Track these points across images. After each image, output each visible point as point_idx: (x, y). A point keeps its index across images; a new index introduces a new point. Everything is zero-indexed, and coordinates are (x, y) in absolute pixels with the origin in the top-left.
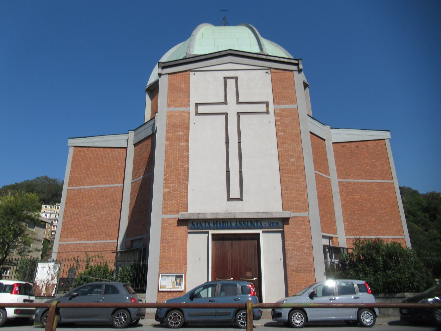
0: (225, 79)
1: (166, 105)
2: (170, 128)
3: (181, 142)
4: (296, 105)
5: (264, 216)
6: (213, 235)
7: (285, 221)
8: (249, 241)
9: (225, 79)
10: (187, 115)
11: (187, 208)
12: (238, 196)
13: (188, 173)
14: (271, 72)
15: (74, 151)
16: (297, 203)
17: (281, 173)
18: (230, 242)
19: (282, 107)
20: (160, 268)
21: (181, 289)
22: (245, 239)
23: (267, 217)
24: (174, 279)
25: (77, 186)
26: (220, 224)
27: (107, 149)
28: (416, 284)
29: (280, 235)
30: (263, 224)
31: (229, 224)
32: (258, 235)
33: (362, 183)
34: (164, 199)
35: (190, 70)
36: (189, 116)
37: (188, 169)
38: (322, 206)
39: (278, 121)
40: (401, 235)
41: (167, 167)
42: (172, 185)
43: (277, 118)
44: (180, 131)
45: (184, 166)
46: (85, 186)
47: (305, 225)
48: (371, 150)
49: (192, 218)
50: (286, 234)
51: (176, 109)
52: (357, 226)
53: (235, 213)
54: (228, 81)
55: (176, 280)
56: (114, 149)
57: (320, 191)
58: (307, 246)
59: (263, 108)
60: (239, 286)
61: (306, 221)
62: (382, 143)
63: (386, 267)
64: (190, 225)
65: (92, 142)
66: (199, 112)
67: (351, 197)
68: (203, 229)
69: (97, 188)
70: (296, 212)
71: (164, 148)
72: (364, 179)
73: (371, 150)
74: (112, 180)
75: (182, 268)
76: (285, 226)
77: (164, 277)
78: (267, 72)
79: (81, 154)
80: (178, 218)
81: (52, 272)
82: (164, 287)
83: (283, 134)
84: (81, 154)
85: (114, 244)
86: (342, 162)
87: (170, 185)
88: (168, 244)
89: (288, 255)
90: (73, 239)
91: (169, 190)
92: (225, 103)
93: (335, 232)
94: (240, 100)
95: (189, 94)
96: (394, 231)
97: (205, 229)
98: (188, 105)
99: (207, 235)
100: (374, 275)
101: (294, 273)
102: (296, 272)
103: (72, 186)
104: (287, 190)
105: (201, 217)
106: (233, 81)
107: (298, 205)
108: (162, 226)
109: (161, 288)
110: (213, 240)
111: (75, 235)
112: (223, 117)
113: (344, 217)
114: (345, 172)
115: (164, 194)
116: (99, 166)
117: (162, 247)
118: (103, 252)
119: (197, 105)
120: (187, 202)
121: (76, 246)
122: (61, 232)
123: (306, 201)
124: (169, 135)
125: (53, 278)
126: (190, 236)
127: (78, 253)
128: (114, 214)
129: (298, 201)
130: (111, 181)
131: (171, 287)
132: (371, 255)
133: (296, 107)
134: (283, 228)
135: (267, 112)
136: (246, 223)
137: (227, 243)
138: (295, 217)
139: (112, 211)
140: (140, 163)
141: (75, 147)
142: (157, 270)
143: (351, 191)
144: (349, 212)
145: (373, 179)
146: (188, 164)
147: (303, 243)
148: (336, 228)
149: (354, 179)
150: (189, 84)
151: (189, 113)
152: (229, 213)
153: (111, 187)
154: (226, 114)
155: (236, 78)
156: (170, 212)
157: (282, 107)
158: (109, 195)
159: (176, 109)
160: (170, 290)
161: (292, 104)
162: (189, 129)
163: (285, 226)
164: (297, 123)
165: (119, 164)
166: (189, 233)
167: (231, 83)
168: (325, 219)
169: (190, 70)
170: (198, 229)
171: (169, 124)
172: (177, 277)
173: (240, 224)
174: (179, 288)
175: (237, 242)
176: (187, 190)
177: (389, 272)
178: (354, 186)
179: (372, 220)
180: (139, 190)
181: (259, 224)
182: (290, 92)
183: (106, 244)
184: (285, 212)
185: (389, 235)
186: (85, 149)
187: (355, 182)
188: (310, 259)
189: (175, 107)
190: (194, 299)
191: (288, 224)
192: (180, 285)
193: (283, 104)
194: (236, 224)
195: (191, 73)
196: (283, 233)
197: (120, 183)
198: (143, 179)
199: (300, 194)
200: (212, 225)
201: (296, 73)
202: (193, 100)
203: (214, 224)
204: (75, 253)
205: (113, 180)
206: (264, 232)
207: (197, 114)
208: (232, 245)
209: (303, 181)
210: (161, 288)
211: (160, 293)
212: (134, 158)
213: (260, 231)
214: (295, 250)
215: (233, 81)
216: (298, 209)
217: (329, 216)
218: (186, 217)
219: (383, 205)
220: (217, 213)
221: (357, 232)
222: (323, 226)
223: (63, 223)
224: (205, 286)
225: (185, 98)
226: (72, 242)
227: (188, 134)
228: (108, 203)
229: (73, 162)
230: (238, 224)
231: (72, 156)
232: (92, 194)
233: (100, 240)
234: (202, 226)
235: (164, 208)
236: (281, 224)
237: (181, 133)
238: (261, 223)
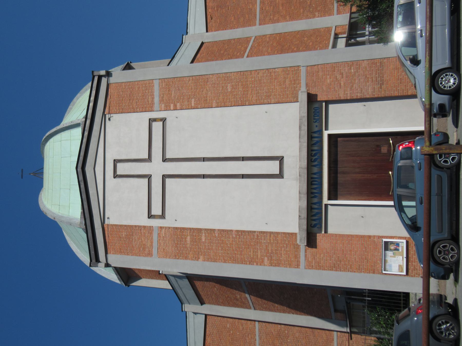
1: (148, 259)
3: (201, 239)
4: (154, 81)
5: (305, 128)
6: (329, 199)
8: (339, 149)
10: (163, 230)
11: (292, 234)
13: (243, 232)
16: (287, 82)
17: (247, 103)
18: (339, 175)
19: (156, 100)
20: (374, 273)
21: (403, 244)
22: (336, 155)
23: (306, 124)
24: (389, 253)
26: (315, 189)
29: (331, 106)
30: (316, 129)
31: (315, 176)
32: (330, 136)
34: (278, 264)
35: (103, 223)
36: (166, 228)
37: (237, 231)
38: (293, 47)
39: (175, 106)
41: (235, 260)
43: (172, 107)
44: (186, 241)
45: (234, 236)
47: (318, 72)
49: (305, 227)
50: (330, 98)
51: (155, 244)
53: (300, 168)
54: (118, 173)
55: (391, 250)
56: (208, 333)
57: (271, 50)
59: (157, 126)
60: (401, 163)
64: (315, 229)
67: (281, 8)
68: (322, 213)
70: (300, 83)
71: (207, 264)
75: (374, 242)
76: (319, 99)
77: (387, 267)
78: (109, 119)
80: (305, 246)
82: (400, 267)
83: (193, 100)
85: (339, 336)
86: (233, 19)
87: (259, 256)
88: (341, 262)
89: (359, 96)
91: (266, 258)
92: (149, 177)
93: (328, 30)
94: (146, 157)
95: (136, 226)
97: (321, 209)
98: (150, 229)
99: (329, 206)
101: (384, 87)
104: (269, 96)
105: (304, 215)
106: (119, 165)
107: (291, 81)
109: (402, 271)
110: (336, 199)
112: (168, 180)
113: (307, 17)
114: (247, 16)
119: (150, 216)
120: (284, 233)
123: (285, 69)
126: (331, 230)
129: (285, 82)
130: (251, 338)
131: (401, 257)
133: (158, 81)
134: (322, 102)
135: (164, 120)
136: (314, 152)
137: (341, 179)
138: (307, 85)
139: (294, 337)
140: (228, 297)
142: (376, 276)
143: (272, 7)
144: (302, 10)
146: (231, 231)
148: (323, 28)
150: (121, 226)
152: (300, 176)
153: (260, 338)
154: (164, 177)
155: (116, 162)
156: (297, 257)
157: (156, 100)
158: (271, 342)
159: (155, 244)
160: (405, 259)
161: (153, 86)
162: (184, 229)
163: (319, 99)
164: (179, 81)
165: (228, 326)
166: (326, 232)
167: (122, 169)
168: (311, 44)
169: (103, 223)
170: (321, 218)
171: (176, 256)
172: (386, 248)
173: (315, 160)
174: (402, 247)
175: (339, 165)
176: (267, 232)
180: (265, 299)
181: (315, 135)
182: (136, 89)
188: (365, 64)
189: (152, 245)
190: (419, 225)
191: (316, 95)
192: (398, 244)
193: (153, 98)
194: (315, 166)
196: (328, 103)
197: (255, 326)
198: (250, 294)
199: (275, 79)
200: (315, 200)
201: (112, 80)
202: (144, 221)
203: (315, 197)
205: (250, 335)
206: (327, 129)
207: (163, 216)
208: (344, 173)
209: (258, 73)
210: (402, 271)
211: (409, 273)
212: (221, 305)
213: (326, 134)
214: (352, 86)
215: (119, 165)
216: (296, 81)
217: (306, 39)
218: (304, 235)
220: (300, 193)
222: (319, 46)
224: (400, 209)
225: (141, 233)
227: (190, 229)
230: (316, 163)
234: (317, 213)
235: (290, 266)
236: (316, 105)
237: (188, 239)
238: (315, 132)
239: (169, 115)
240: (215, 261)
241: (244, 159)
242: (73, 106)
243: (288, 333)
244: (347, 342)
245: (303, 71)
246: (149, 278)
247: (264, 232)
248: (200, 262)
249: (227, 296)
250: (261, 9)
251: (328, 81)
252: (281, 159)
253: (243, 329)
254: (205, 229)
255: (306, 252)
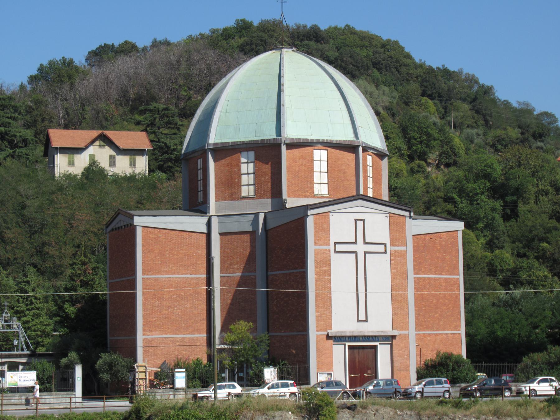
0: (356, 220)
2: (318, 264)
3: (326, 276)
4: (405, 247)
7: (394, 337)
8: (369, 350)
9: (356, 220)
12: (364, 319)
14: (390, 216)
15: (143, 231)
16: (402, 324)
18: (357, 350)
19: (396, 248)
22: (367, 349)
25: (153, 274)
27: (183, 232)
28: (468, 379)
30: (379, 339)
33: (431, 279)
35: (330, 212)
36: (330, 254)
37: (331, 298)
39: (393, 260)
40: (459, 330)
42: (321, 310)
43: (392, 258)
44: (324, 267)
46: (162, 275)
47: (406, 340)
48: (444, 243)
49: (337, 335)
50: (394, 346)
52: (423, 321)
54: (358, 222)
58: (406, 354)
61: (407, 337)
62: (455, 235)
63: (454, 369)
64: (334, 339)
65: (165, 223)
66: (337, 250)
69: (177, 278)
70: (401, 330)
71: (314, 280)
72: (433, 275)
73: (444, 243)
74: (193, 270)
78: (386, 216)
79: (152, 236)
81: (273, 374)
84: (152, 236)
89: (394, 360)
90: (157, 332)
91: (319, 314)
92: (356, 243)
95: (329, 234)
96: (453, 326)
97: (343, 341)
98: (328, 244)
100: (446, 374)
101: (398, 371)
102: (399, 370)
103: (147, 275)
105: (343, 334)
106: (362, 222)
108: (317, 340)
110: (348, 349)
111: (159, 328)
112: (354, 255)
115: (317, 317)
116: (175, 253)
117: (317, 355)
118: (192, 347)
121: (163, 340)
122: (143, 325)
123: (408, 323)
124: (317, 270)
125: (274, 378)
126: (334, 346)
127: (165, 347)
128: (200, 307)
130: (192, 271)
132: (446, 362)
134: (392, 342)
135: (385, 252)
137: (356, 351)
141: (143, 227)
145: (442, 275)
147: (404, 351)
149: (425, 274)
150: (329, 224)
151: (330, 251)
153: (192, 278)
154: (356, 253)
155: (363, 220)
156: (321, 330)
157: (396, 248)
162: (330, 266)
163: (394, 340)
165: (199, 252)
166: (334, 344)
167: (360, 224)
169: (330, 212)
170: (338, 341)
172: (328, 374)
173: (365, 338)
175: (361, 350)
177: (455, 372)
178: (424, 282)
179: (436, 316)
181: (377, 339)
183: (195, 338)
184: (394, 331)
185: (448, 330)
186: (156, 231)
187: (425, 278)
188: (408, 362)
189: (320, 245)
195: (331, 214)
198: (241, 276)
200: (347, 339)
201: (407, 219)
202: (333, 240)
203: (348, 338)
204: (162, 347)
206: (380, 344)
208: (359, 353)
212: (220, 249)
213: (377, 343)
215: (362, 222)
216: (402, 329)
219: (447, 301)
220: (353, 332)
221: (422, 328)
223: (143, 316)
226: (157, 336)
227: (330, 269)
228: (191, 295)
229: (143, 246)
231: (141, 238)
232: (172, 285)
233: (188, 334)
234: (341, 340)
235: (317, 327)
236: (390, 339)
237: (325, 268)
239: (388, 256)
240: (316, 285)
241: (366, 301)
242: (353, 88)
243: (200, 300)
244: (200, 344)
245: (406, 332)
246: (215, 171)
247: (331, 312)
248: (314, 276)
249: (234, 257)
250: (421, 278)
251: (402, 345)
252: (366, 321)
253: (198, 264)
254: (330, 279)
255: (324, 335)
